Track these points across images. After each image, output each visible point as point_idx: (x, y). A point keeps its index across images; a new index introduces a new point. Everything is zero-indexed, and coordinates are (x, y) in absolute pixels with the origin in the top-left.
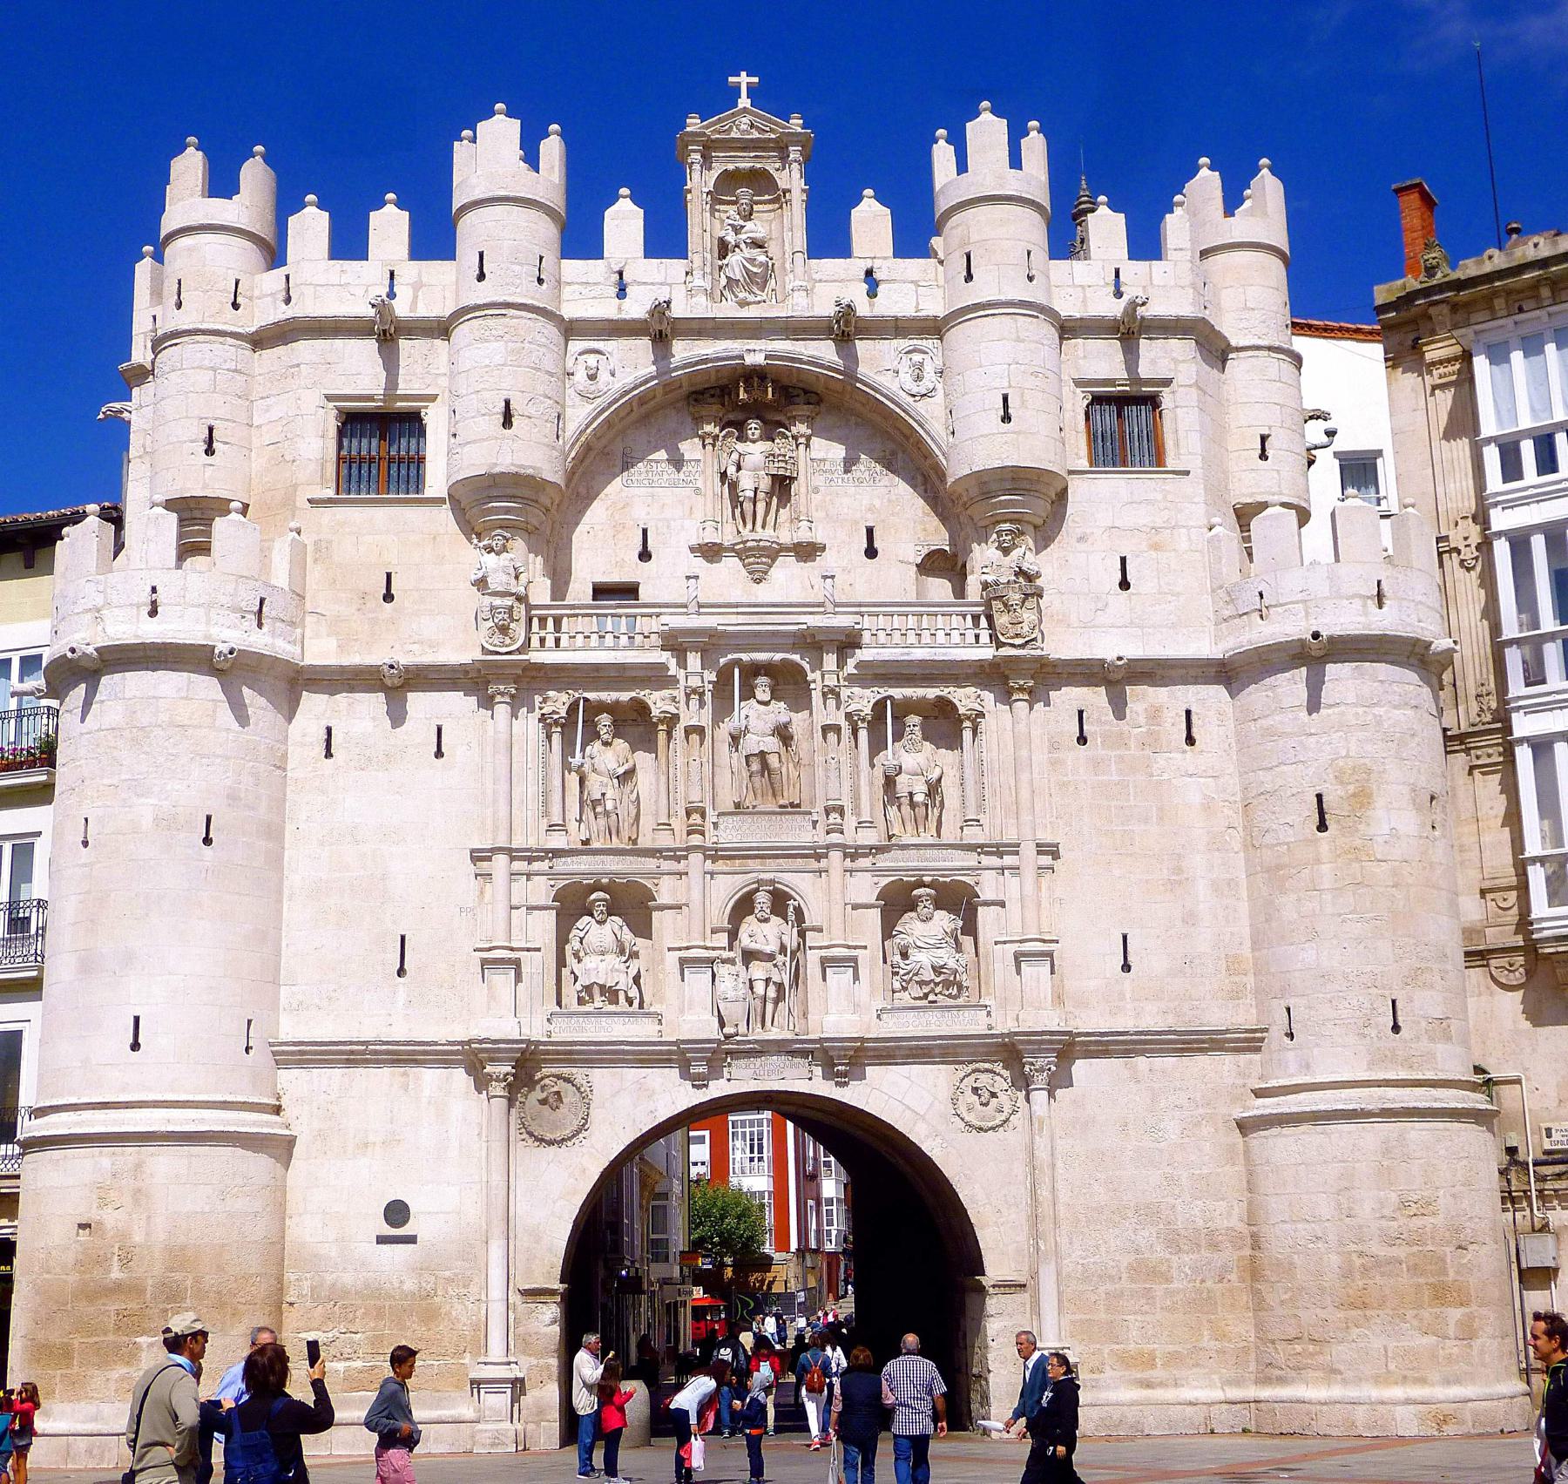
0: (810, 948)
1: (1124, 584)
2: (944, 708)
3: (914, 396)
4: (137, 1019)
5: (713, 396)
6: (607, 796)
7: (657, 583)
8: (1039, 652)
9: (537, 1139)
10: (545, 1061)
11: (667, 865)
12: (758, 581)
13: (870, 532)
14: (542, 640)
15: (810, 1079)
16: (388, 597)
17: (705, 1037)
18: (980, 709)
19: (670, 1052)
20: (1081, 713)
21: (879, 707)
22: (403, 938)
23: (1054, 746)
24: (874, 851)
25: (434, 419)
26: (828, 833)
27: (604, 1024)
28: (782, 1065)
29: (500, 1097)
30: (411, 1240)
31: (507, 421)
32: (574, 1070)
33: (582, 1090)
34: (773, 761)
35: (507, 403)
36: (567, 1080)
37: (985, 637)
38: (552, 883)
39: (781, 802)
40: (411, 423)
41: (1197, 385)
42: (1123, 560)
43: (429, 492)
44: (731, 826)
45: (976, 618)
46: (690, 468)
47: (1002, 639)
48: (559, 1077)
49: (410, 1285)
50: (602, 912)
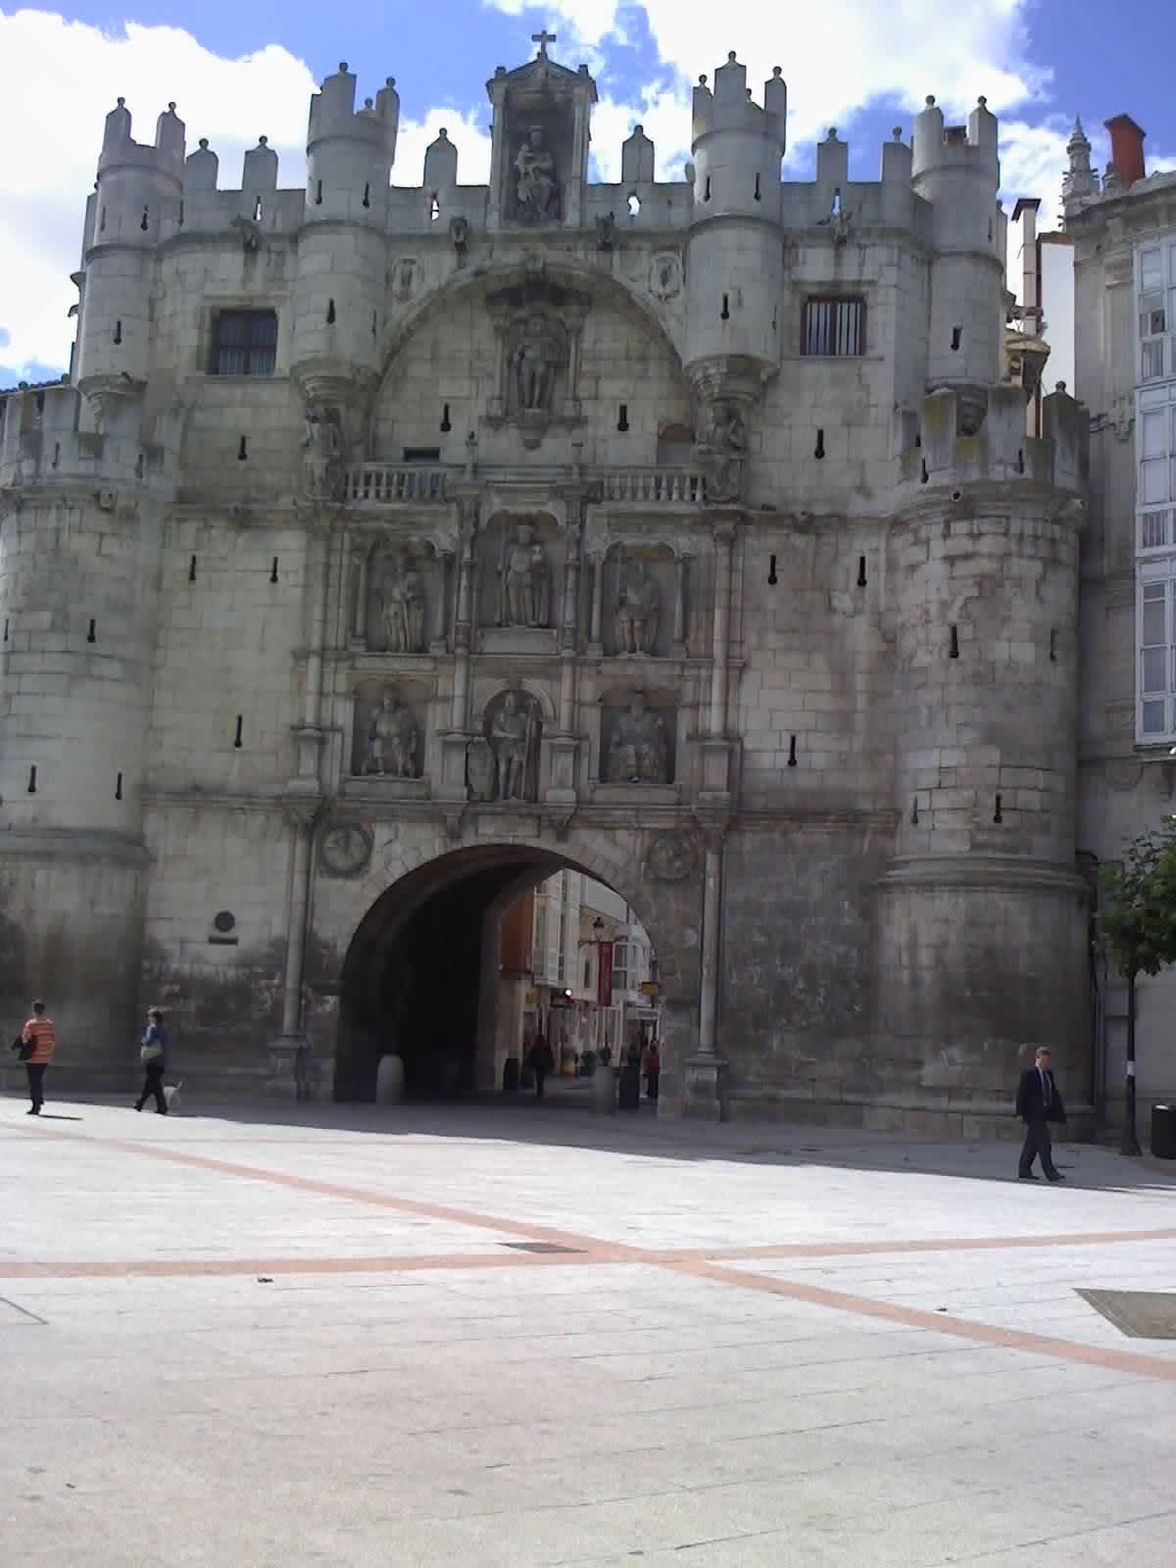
1: (820, 453)
2: (664, 551)
3: (660, 297)
4: (34, 770)
7: (454, 449)
12: (532, 448)
13: (623, 410)
14: (355, 493)
15: (538, 836)
16: (243, 456)
21: (615, 547)
22: (240, 719)
25: (283, 315)
30: (234, 941)
31: (331, 318)
35: (332, 304)
37: (698, 497)
39: (534, 623)
40: (269, 316)
41: (895, 286)
42: (821, 434)
43: (276, 374)
45: (694, 482)
47: (712, 498)
49: (231, 973)
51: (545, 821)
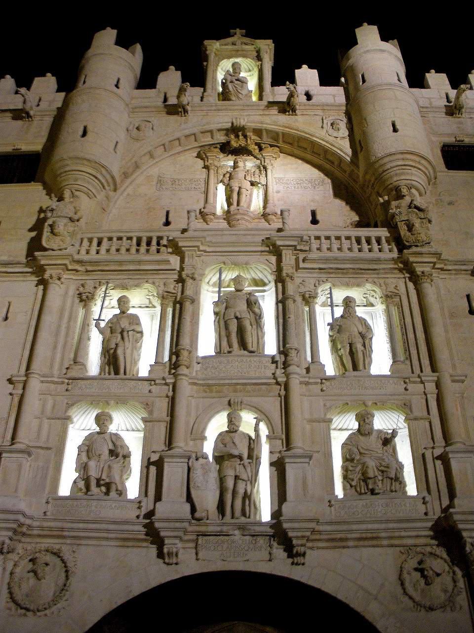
5: (216, 147)
6: (121, 343)
8: (433, 250)
13: (314, 213)
15: (270, 560)
17: (177, 516)
18: (397, 292)
20: (468, 296)
23: (452, 315)
31: (84, 134)
34: (247, 323)
36: (57, 554)
44: (211, 366)
46: (199, 182)
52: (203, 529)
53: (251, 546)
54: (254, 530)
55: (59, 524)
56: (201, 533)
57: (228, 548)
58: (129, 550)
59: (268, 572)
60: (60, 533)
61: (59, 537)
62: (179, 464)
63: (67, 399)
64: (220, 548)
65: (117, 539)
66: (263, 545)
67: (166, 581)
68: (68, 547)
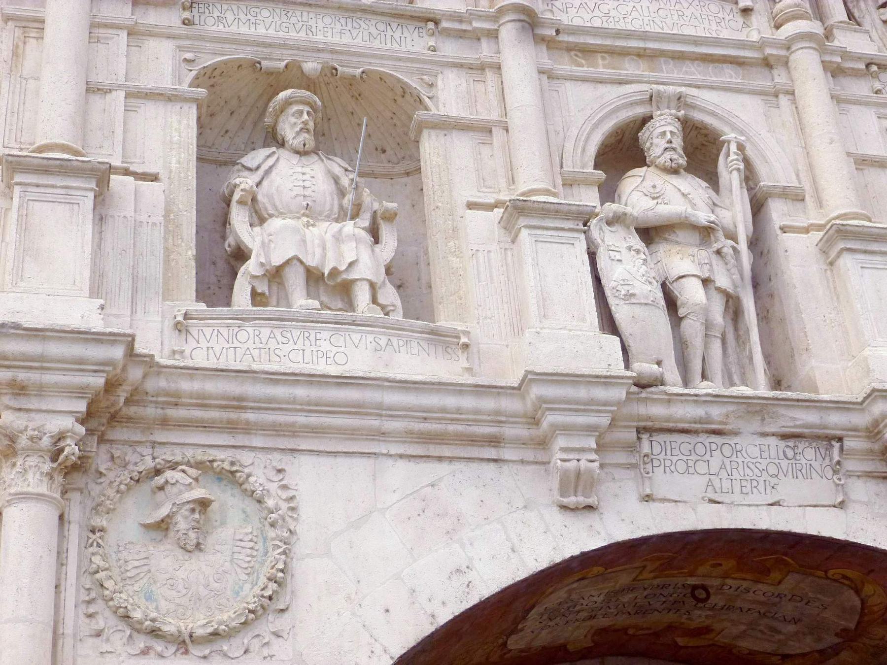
0: (784, 229)
9: (136, 628)
10: (165, 423)
11: (450, 50)
15: (841, 505)
19: (499, 418)
24: (874, 68)
26: (778, 27)
27: (325, 346)
28: (773, 470)
29: (39, 497)
32: (246, 457)
33: (270, 503)
38: (189, 56)
48: (204, 467)
50: (305, 129)
51: (853, 453)
52: (657, 411)
53: (784, 463)
54: (794, 419)
55: (233, 388)
56: (649, 424)
57: (723, 466)
58: (444, 468)
59: (838, 534)
60: (233, 415)
61: (232, 427)
62: (561, 234)
63: (180, 48)
64: (702, 467)
65: (410, 433)
66: (816, 465)
67: (567, 555)
68: (262, 457)
